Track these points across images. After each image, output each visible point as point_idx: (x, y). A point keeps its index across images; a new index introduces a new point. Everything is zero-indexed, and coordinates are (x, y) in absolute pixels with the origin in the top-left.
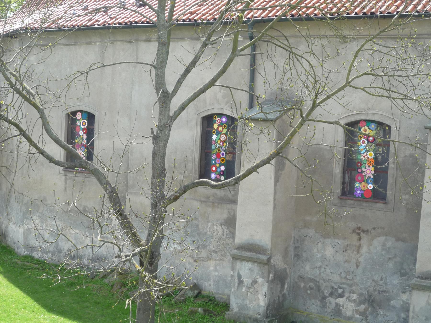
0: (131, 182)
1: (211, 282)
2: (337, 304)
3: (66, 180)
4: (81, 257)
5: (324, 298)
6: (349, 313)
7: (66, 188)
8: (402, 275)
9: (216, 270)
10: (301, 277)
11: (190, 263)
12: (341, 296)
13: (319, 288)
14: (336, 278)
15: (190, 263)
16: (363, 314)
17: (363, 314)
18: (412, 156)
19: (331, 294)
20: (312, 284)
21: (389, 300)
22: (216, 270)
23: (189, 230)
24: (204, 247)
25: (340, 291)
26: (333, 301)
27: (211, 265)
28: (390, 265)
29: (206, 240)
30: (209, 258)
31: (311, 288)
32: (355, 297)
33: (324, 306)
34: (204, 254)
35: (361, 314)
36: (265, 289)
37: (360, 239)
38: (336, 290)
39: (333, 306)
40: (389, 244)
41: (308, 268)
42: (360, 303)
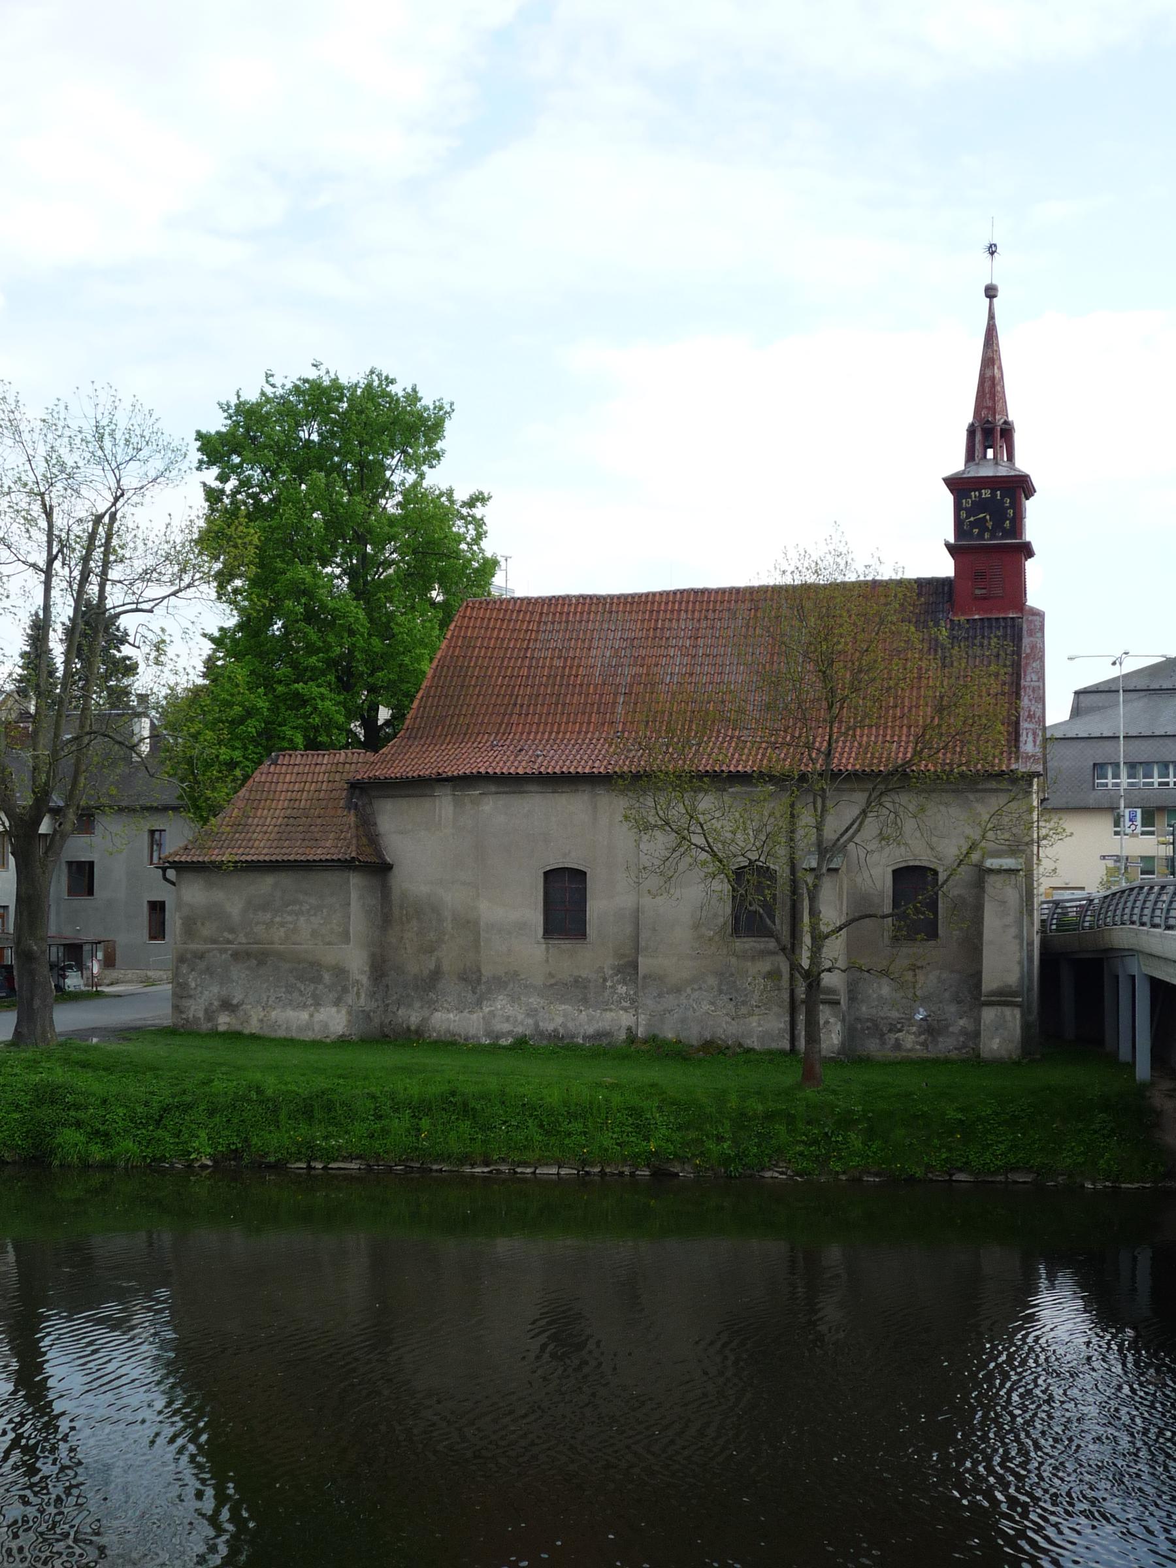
0: (642, 944)
1: (755, 1039)
2: (897, 1039)
3: (547, 950)
4: (573, 1037)
5: (882, 1035)
6: (909, 1046)
7: (547, 961)
8: (958, 1003)
9: (760, 1025)
10: (858, 1019)
11: (727, 1023)
12: (900, 1031)
13: (876, 1026)
14: (895, 1014)
15: (727, 1023)
16: (924, 1044)
17: (924, 1044)
18: (959, 895)
19: (890, 1031)
20: (869, 1024)
21: (947, 1027)
22: (760, 1025)
23: (724, 988)
24: (744, 1003)
25: (899, 1026)
26: (893, 1036)
27: (753, 1022)
28: (947, 995)
29: (746, 996)
30: (751, 1014)
31: (868, 1028)
32: (914, 1029)
33: (883, 1043)
34: (744, 1010)
35: (922, 1044)
36: (839, 1027)
37: (915, 975)
38: (895, 1025)
39: (893, 1041)
40: (944, 976)
41: (864, 1009)
42: (920, 1034)
